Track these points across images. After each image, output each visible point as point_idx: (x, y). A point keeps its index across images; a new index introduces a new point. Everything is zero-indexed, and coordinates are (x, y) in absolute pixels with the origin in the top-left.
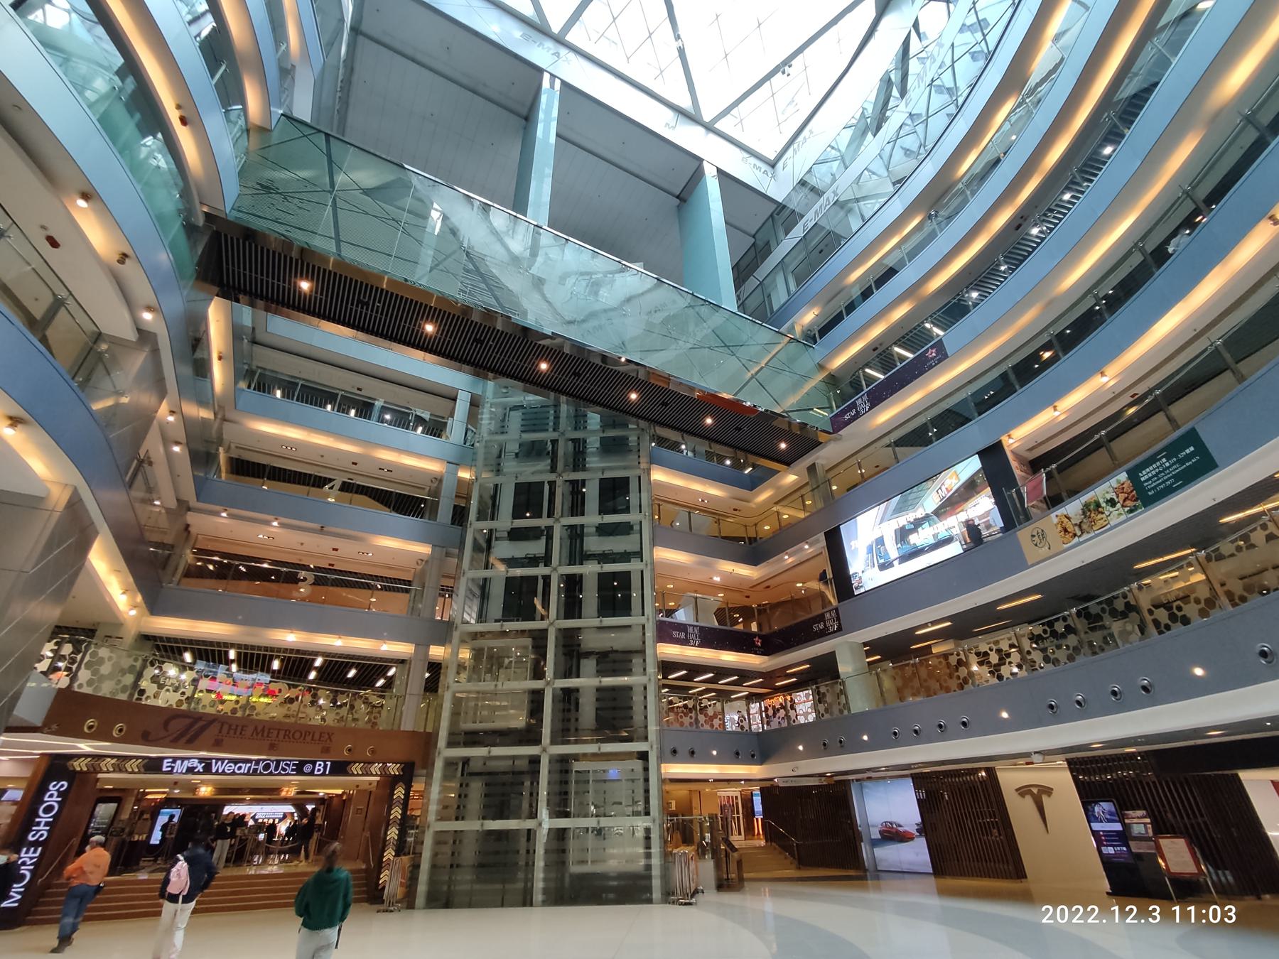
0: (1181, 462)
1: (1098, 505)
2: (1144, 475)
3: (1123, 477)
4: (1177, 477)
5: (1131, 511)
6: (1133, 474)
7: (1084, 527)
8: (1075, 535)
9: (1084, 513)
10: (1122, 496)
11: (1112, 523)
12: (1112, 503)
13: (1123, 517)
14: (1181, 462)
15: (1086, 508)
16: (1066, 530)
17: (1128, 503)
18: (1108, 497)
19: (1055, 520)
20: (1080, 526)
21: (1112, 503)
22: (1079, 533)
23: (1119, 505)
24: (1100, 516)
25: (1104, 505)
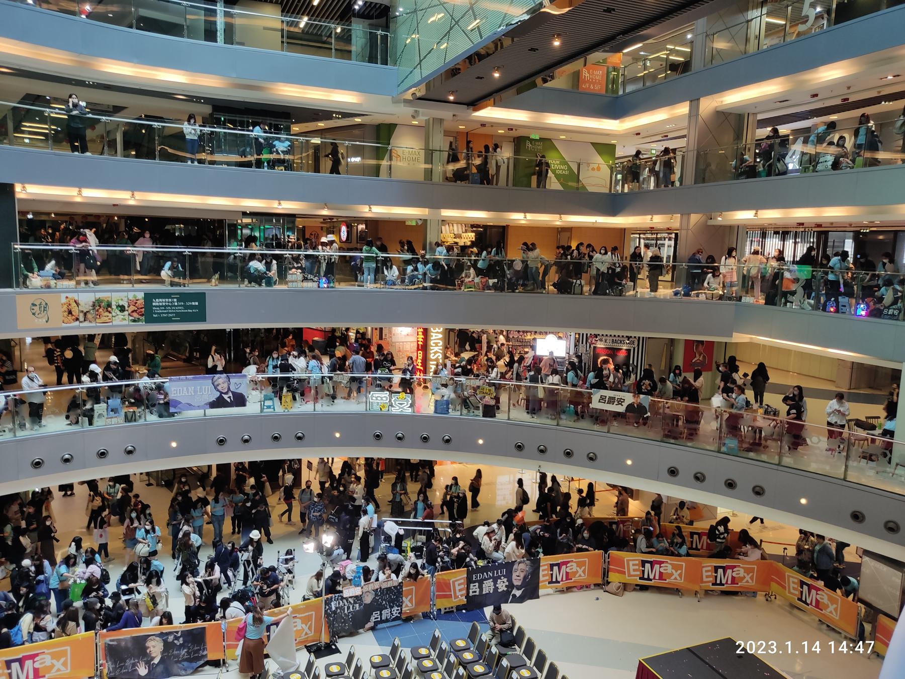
0: (186, 307)
1: (109, 305)
2: (156, 302)
3: (141, 296)
4: (177, 314)
5: (134, 321)
6: (149, 297)
7: (89, 316)
8: (77, 319)
9: (94, 305)
10: (132, 308)
11: (115, 323)
12: (122, 309)
13: (126, 322)
14: (186, 307)
15: (97, 304)
16: (70, 312)
17: (135, 315)
18: (121, 303)
19: (64, 300)
20: (85, 314)
21: (122, 309)
22: (81, 318)
23: (126, 313)
24: (107, 314)
25: (114, 307)
